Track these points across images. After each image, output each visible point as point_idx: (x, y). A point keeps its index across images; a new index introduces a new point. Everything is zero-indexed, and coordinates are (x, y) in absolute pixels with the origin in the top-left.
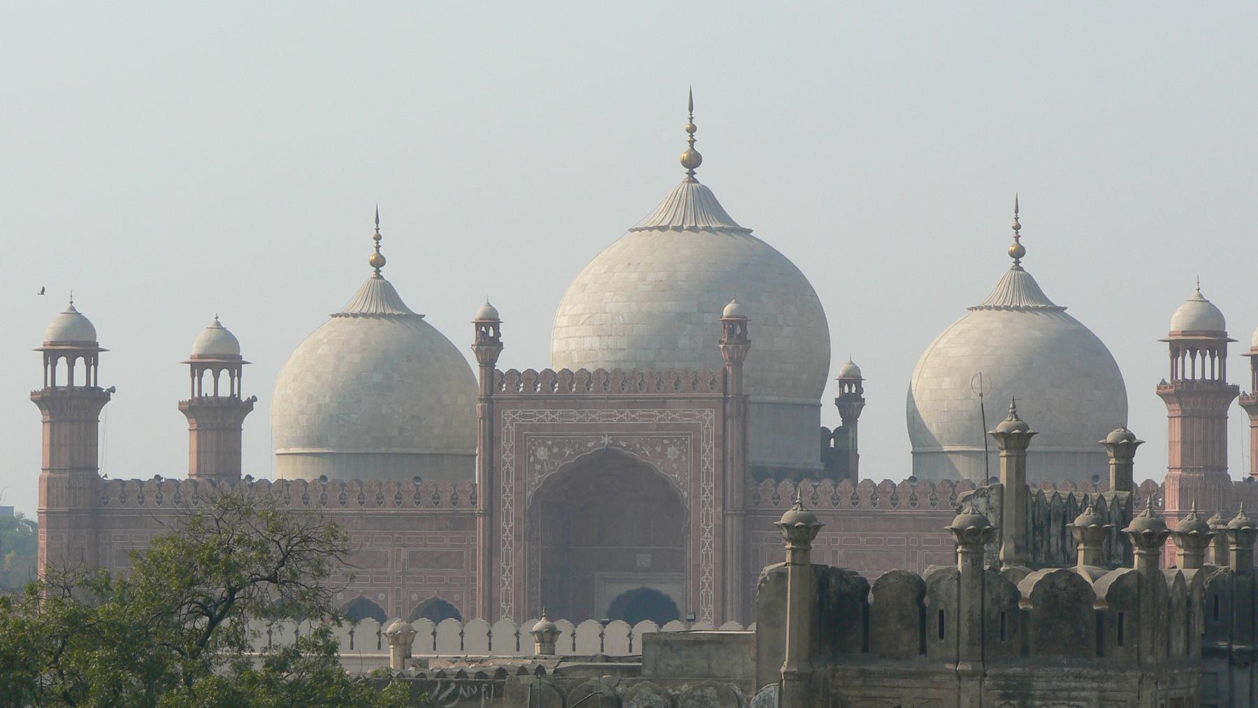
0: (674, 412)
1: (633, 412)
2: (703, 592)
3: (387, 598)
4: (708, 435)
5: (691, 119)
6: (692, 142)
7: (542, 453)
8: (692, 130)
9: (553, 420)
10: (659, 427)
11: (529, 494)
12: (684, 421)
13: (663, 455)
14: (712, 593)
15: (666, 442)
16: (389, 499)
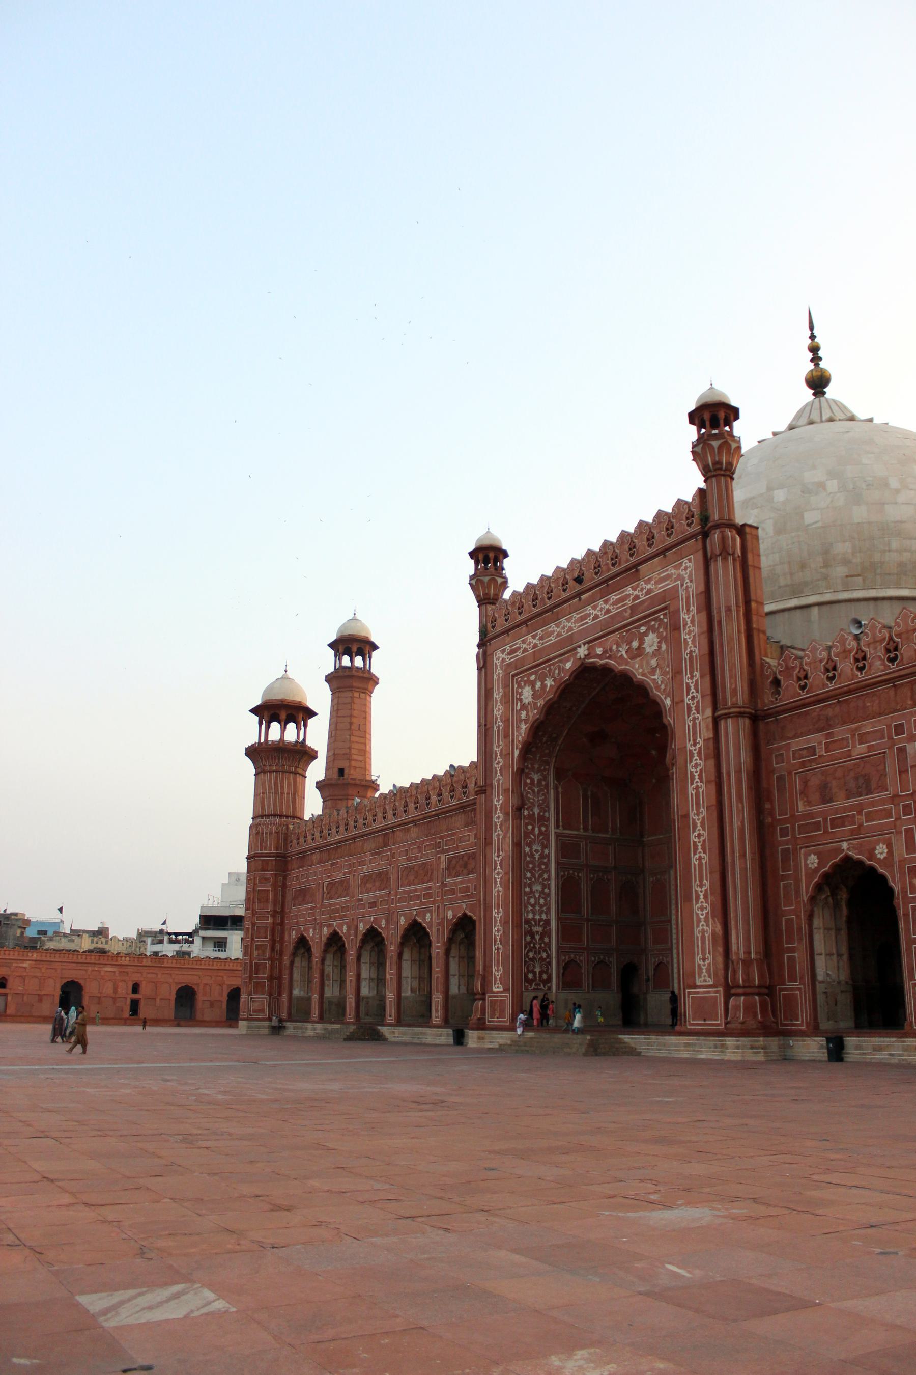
0: (648, 582)
1: (606, 602)
2: (694, 861)
3: (431, 919)
4: (688, 598)
5: (812, 337)
6: (816, 359)
7: (527, 694)
8: (814, 350)
9: (535, 646)
10: (634, 609)
11: (517, 753)
12: (658, 589)
13: (639, 652)
14: (706, 857)
15: (643, 629)
16: (434, 798)
